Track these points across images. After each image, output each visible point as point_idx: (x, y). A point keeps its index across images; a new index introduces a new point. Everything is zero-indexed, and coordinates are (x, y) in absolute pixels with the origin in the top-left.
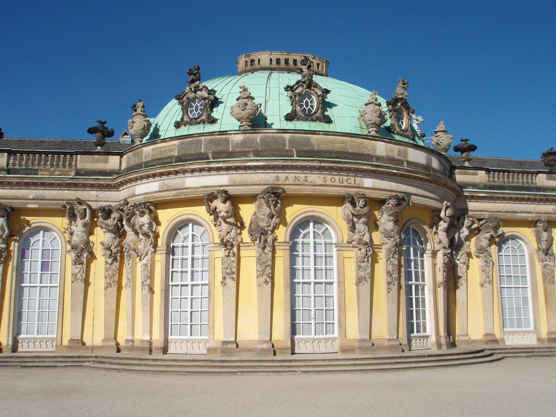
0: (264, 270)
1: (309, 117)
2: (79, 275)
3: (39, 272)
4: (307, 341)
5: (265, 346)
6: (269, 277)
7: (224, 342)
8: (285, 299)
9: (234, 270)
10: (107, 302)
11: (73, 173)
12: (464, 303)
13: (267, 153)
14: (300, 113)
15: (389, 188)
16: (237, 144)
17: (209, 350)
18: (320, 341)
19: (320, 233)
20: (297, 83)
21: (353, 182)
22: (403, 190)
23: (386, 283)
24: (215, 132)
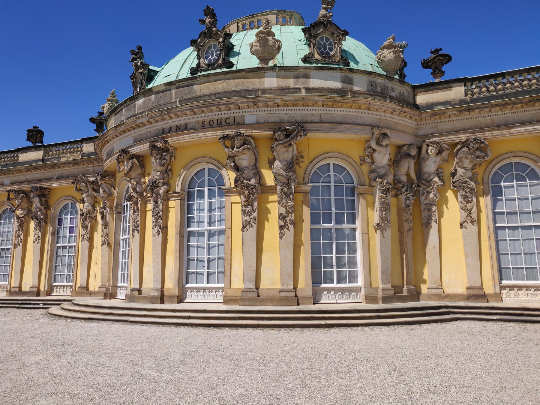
0: (156, 222)
1: (211, 66)
2: (85, 236)
3: (68, 235)
4: (198, 289)
5: (156, 294)
6: (160, 228)
7: (133, 290)
8: (176, 248)
9: (139, 222)
10: (103, 256)
11: (80, 157)
12: (434, 248)
13: (157, 108)
14: (204, 65)
15: (279, 120)
16: (140, 107)
17: (126, 296)
18: (210, 289)
19: (214, 180)
20: (200, 35)
21: (232, 121)
22: (299, 121)
23: (278, 227)
24: (127, 100)
